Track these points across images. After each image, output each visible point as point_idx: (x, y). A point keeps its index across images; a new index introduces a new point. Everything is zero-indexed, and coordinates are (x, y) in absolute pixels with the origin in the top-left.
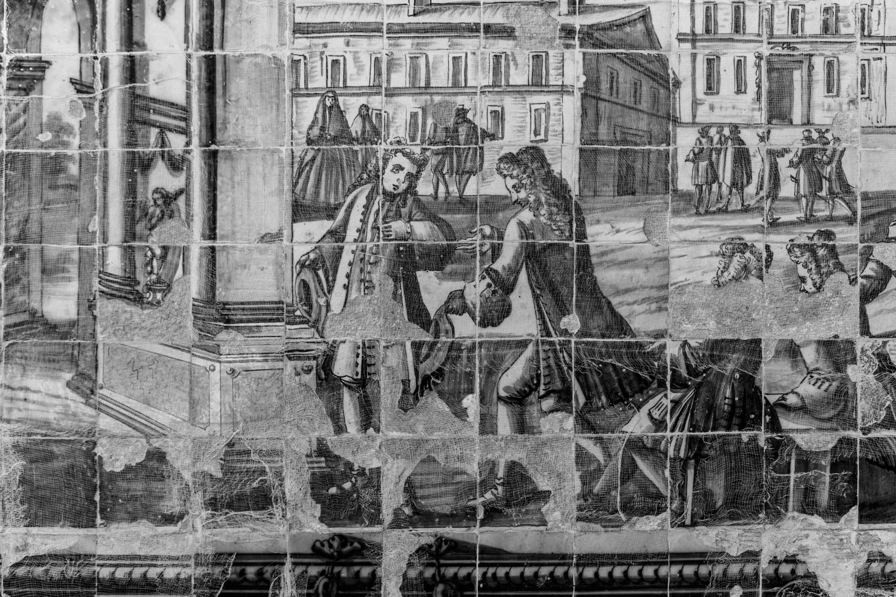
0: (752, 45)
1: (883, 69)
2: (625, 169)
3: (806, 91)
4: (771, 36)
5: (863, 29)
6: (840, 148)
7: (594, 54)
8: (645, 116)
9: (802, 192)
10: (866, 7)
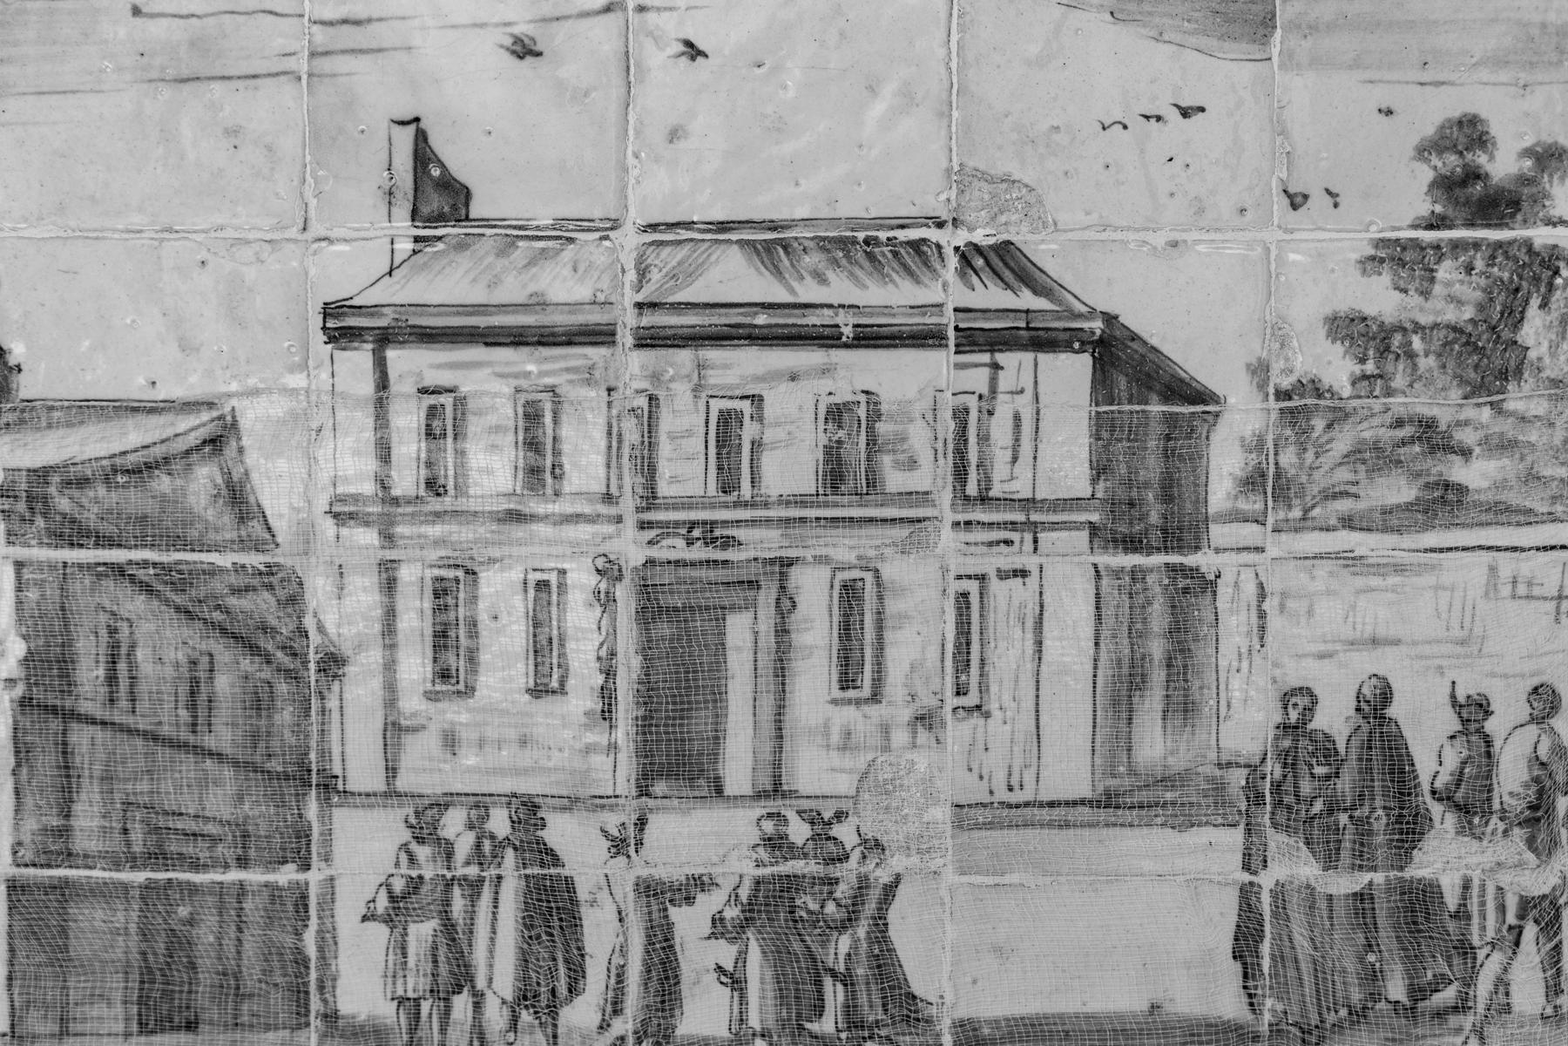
0: (583, 531)
1: (1032, 610)
2: (161, 947)
3: (767, 681)
4: (650, 499)
5: (961, 473)
6: (883, 876)
7: (52, 567)
8: (228, 772)
9: (754, 1022)
10: (972, 402)
